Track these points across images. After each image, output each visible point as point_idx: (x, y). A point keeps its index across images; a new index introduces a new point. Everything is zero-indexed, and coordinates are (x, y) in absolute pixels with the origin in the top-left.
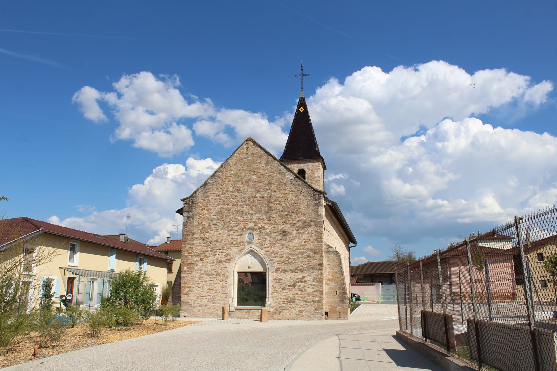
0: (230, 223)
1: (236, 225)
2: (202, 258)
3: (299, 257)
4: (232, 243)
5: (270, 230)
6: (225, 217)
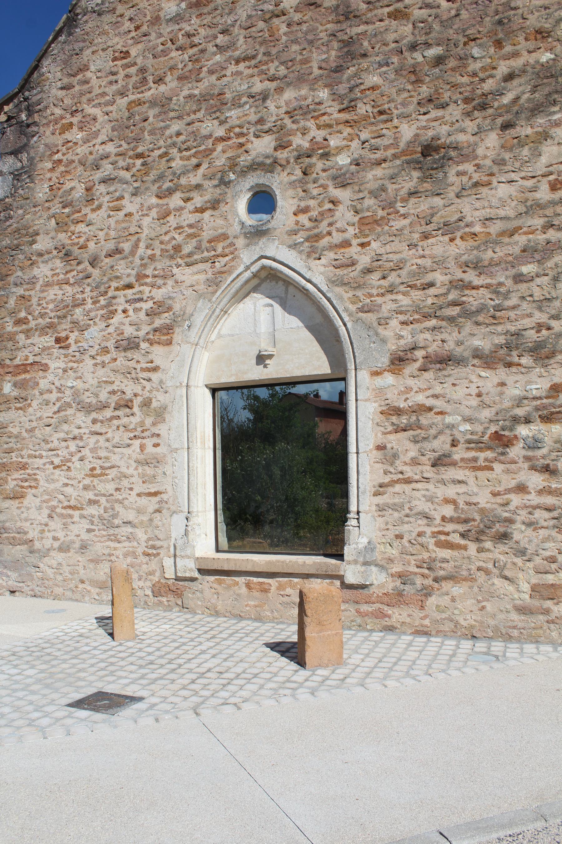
0: (168, 161)
1: (194, 161)
2: (63, 334)
3: (522, 275)
4: (177, 248)
5: (356, 156)
6: (147, 137)
